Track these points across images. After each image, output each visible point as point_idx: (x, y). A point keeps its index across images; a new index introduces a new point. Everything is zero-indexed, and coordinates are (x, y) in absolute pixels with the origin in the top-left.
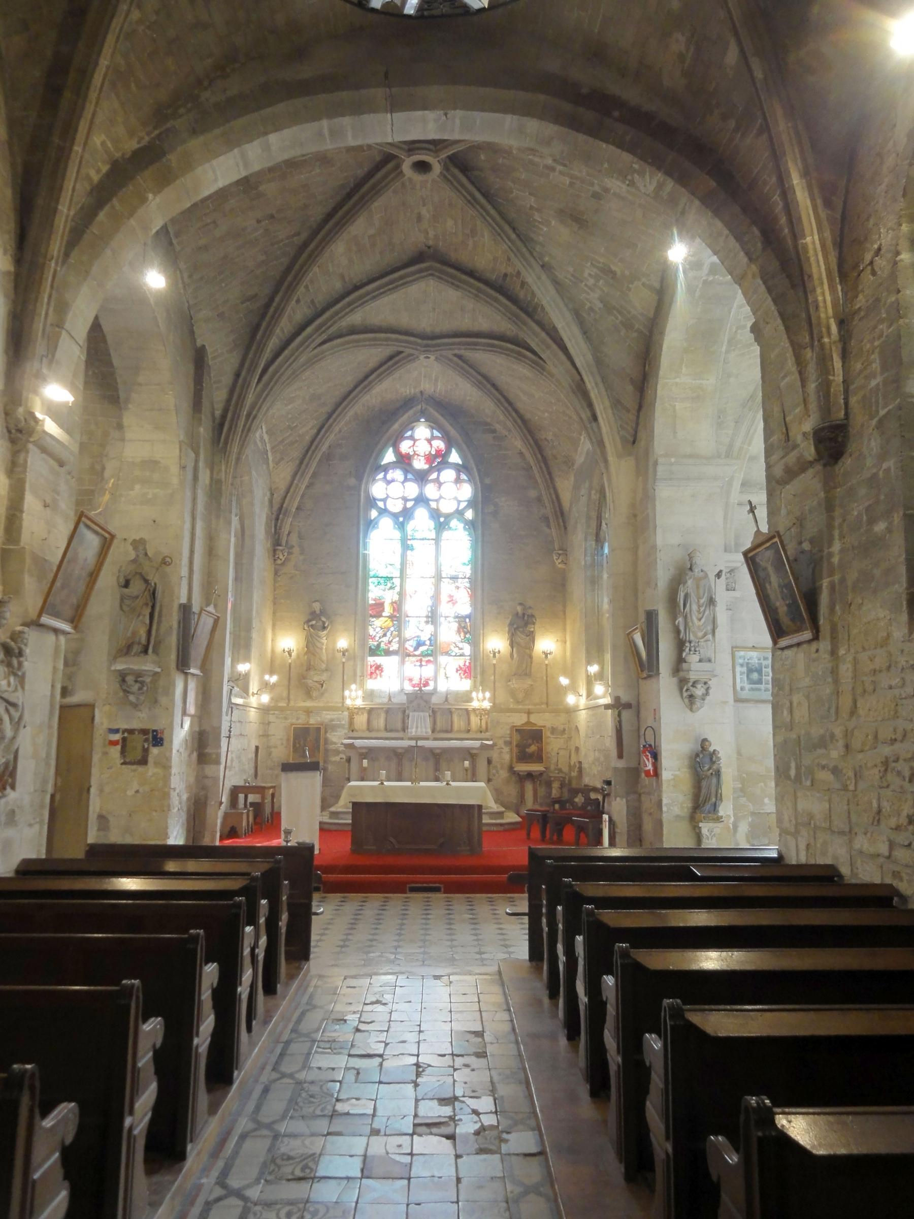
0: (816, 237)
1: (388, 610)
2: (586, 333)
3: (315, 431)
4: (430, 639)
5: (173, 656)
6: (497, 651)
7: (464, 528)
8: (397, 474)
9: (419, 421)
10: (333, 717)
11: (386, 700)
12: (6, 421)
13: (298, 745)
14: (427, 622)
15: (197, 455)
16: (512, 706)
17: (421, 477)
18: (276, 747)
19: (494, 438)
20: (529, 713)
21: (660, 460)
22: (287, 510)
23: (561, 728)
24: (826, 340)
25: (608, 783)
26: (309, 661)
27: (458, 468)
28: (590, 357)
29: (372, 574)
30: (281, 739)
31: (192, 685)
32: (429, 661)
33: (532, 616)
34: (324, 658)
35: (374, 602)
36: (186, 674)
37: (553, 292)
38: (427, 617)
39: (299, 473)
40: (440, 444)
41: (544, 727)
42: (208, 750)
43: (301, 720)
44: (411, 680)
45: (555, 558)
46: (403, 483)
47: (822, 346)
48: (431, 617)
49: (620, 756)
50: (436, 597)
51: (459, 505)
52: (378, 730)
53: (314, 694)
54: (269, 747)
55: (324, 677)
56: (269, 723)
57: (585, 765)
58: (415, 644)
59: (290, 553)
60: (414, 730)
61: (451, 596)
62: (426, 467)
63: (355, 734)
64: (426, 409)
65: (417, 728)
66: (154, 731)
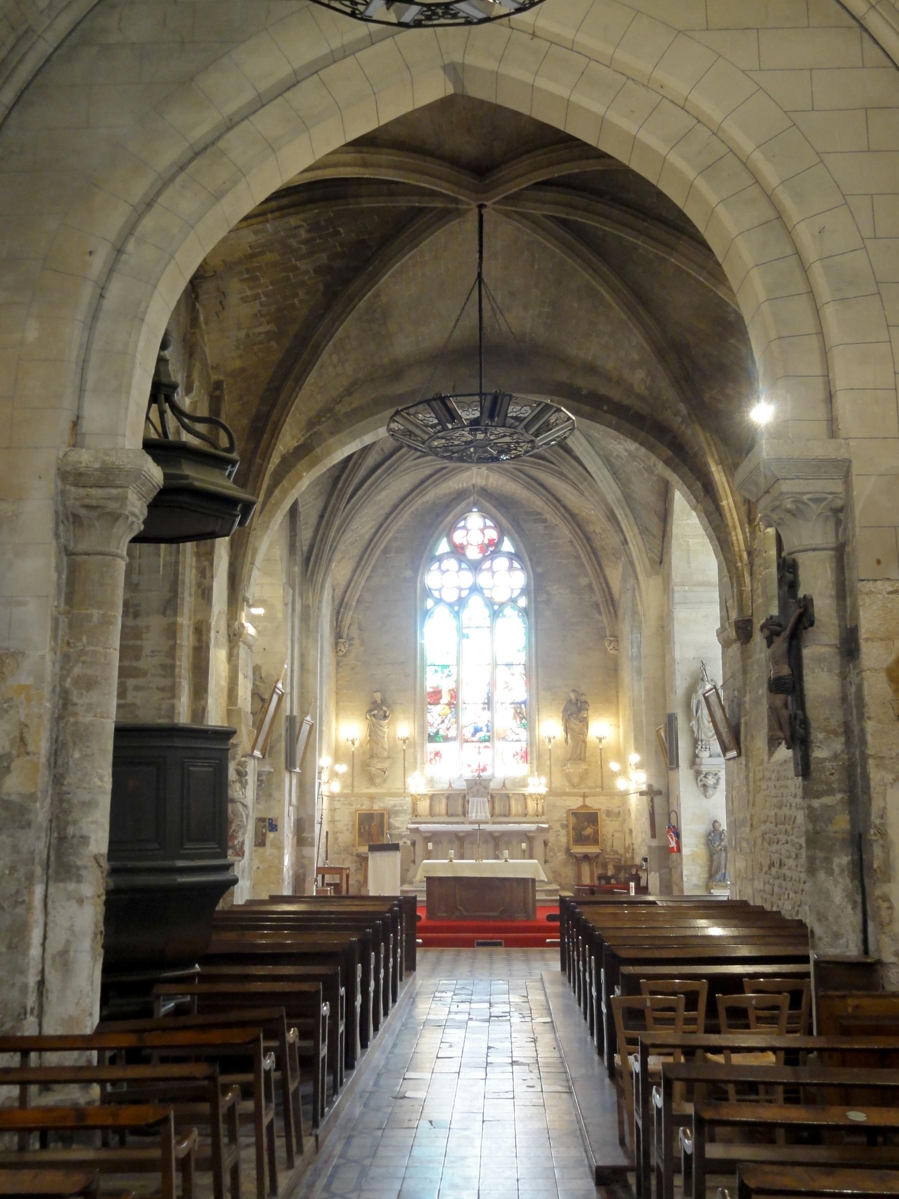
0: (730, 499)
1: (446, 698)
2: (615, 474)
3: (374, 530)
4: (487, 726)
5: (283, 758)
6: (552, 736)
7: (518, 614)
8: (451, 564)
9: (471, 511)
10: (395, 802)
11: (446, 786)
12: (228, 630)
13: (363, 831)
14: (484, 709)
15: (294, 591)
16: (567, 790)
17: (475, 567)
18: (342, 832)
19: (545, 527)
20: (584, 796)
21: (677, 588)
22: (347, 604)
23: (616, 810)
24: (739, 564)
25: (645, 860)
26: (372, 749)
27: (511, 557)
28: (619, 493)
29: (429, 662)
30: (347, 825)
31: (294, 781)
32: (486, 747)
33: (586, 702)
34: (386, 746)
35: (431, 690)
36: (290, 772)
37: (586, 443)
38: (484, 703)
39: (360, 568)
40: (493, 534)
41: (599, 810)
42: (305, 835)
43: (366, 807)
44: (469, 766)
45: (606, 644)
46: (457, 572)
47: (737, 568)
48: (488, 704)
49: (653, 836)
50: (492, 684)
51: (512, 593)
52: (440, 815)
53: (378, 781)
54: (335, 833)
55: (386, 764)
56: (335, 810)
57: (636, 847)
58: (472, 731)
59: (350, 645)
60: (474, 815)
61: (506, 683)
62: (479, 556)
63: (418, 819)
64: (478, 501)
65: (477, 813)
66: (269, 819)
